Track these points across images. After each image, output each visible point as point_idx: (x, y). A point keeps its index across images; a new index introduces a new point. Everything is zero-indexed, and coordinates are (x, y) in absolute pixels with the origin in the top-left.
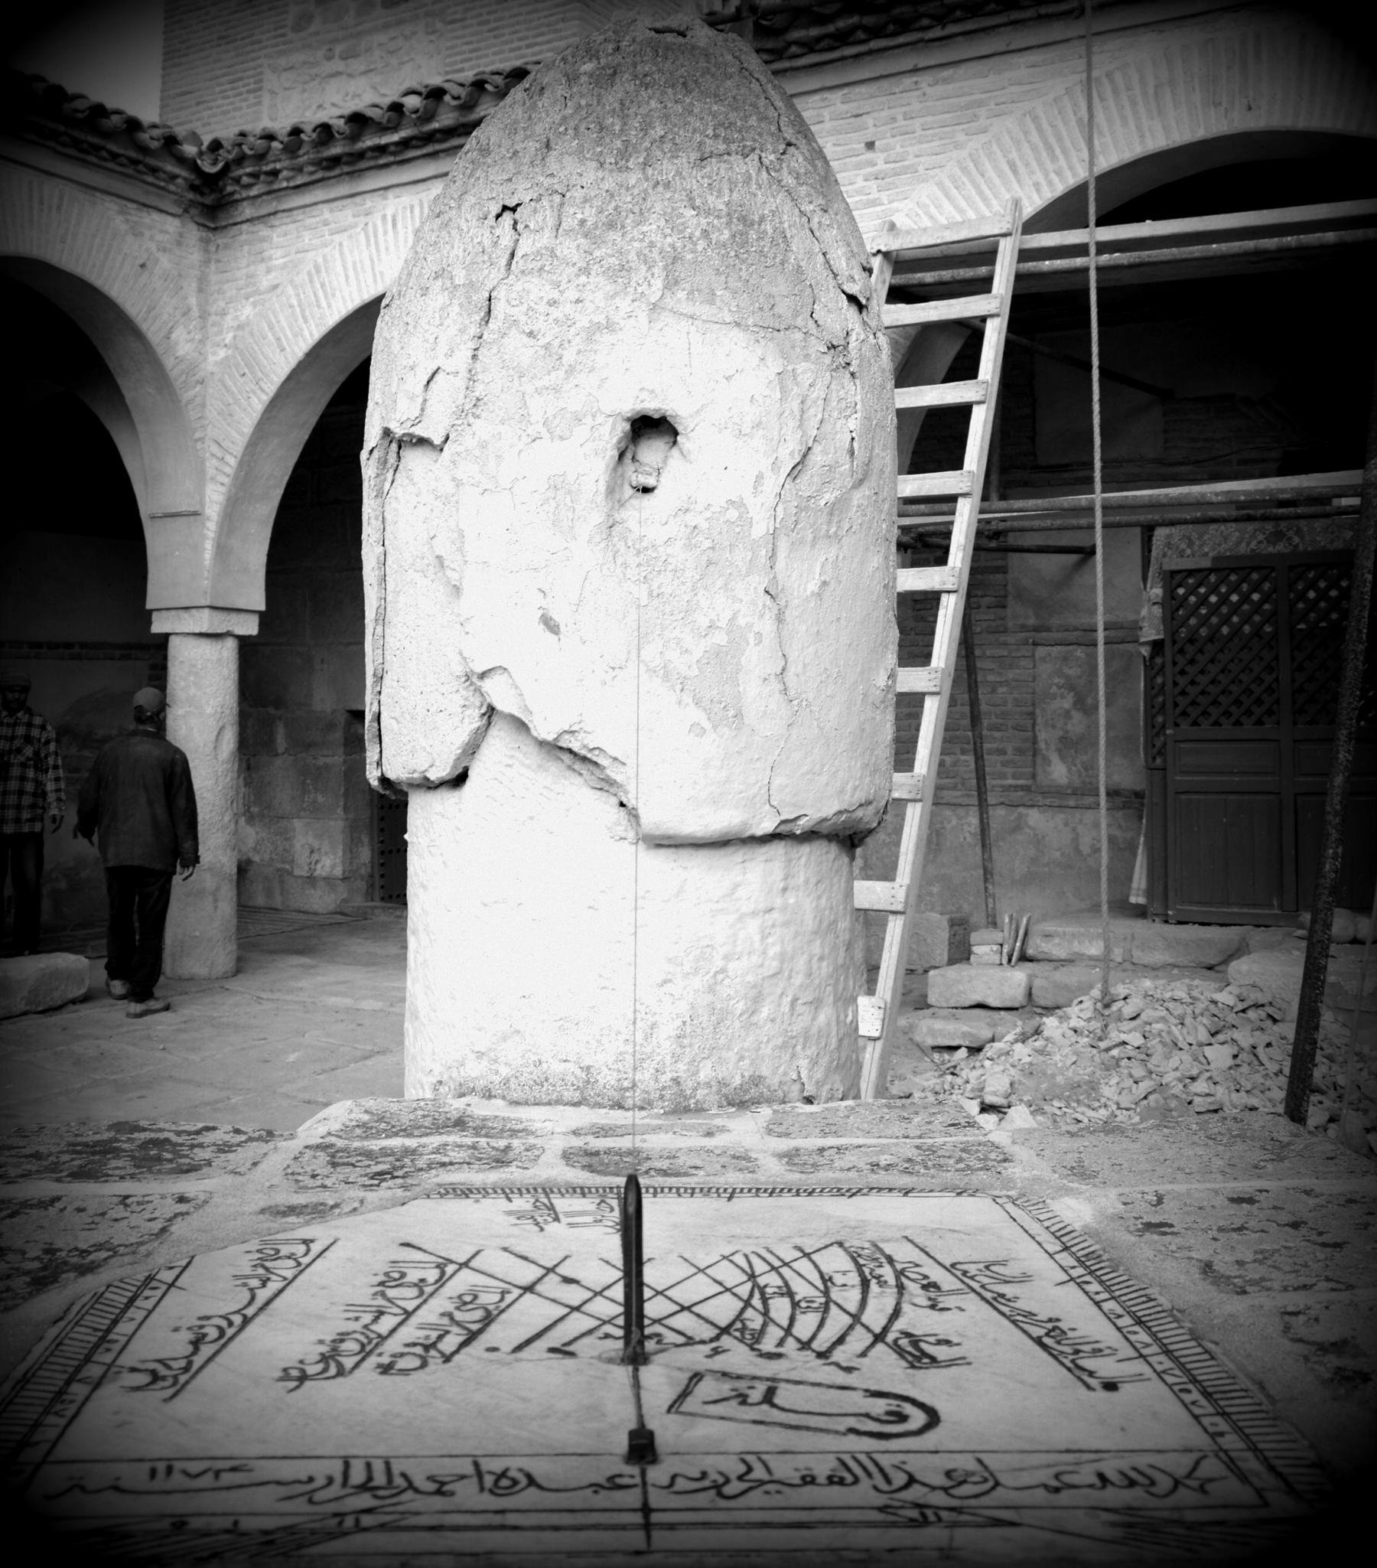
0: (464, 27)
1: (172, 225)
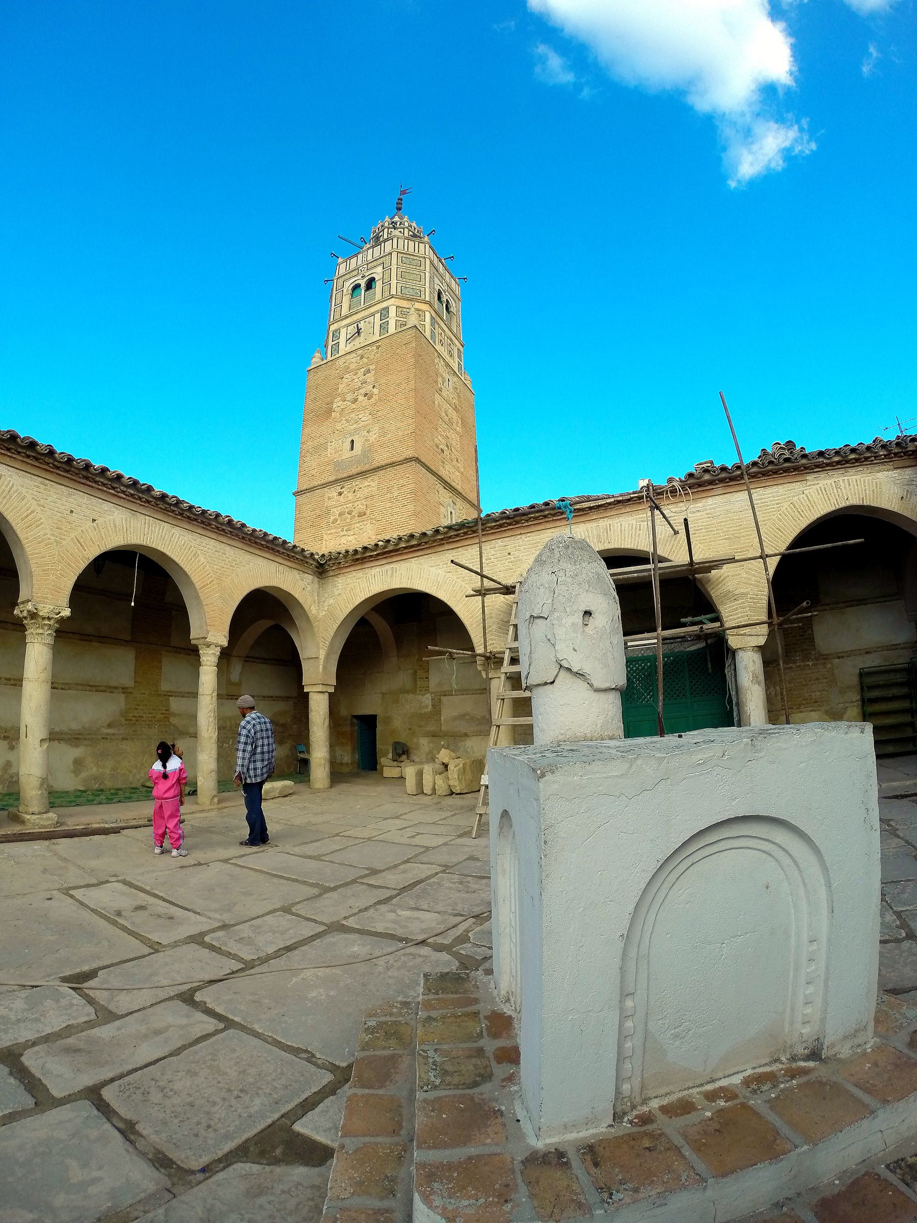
1: (311, 577)
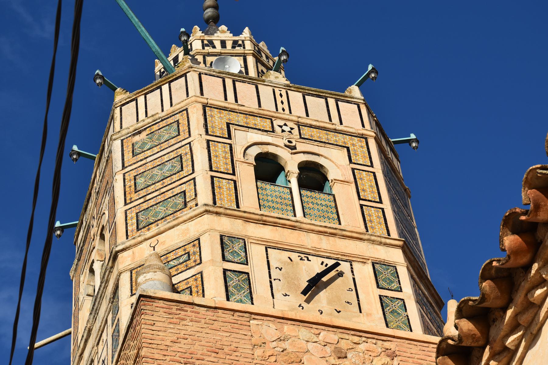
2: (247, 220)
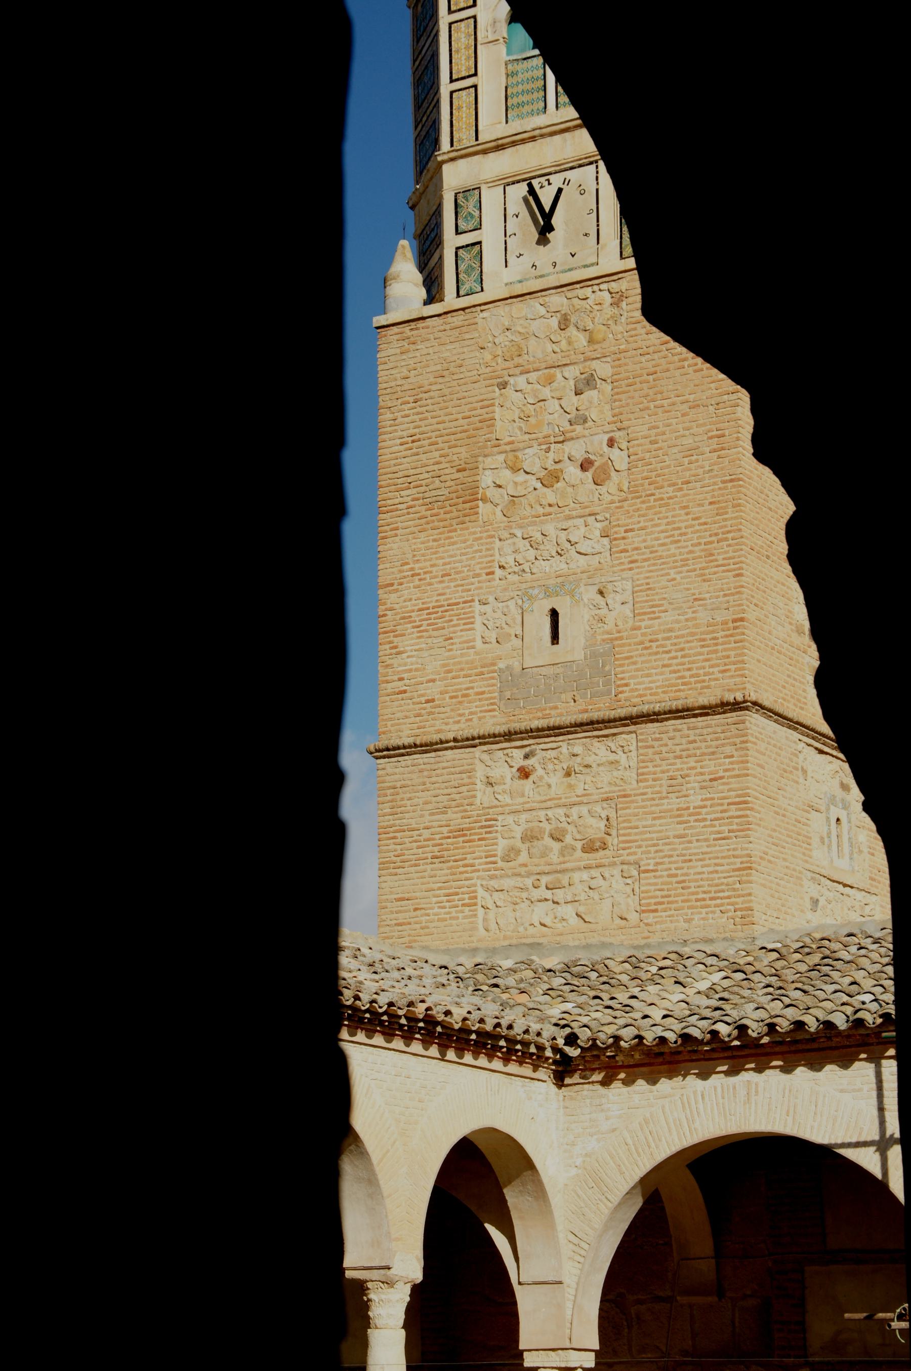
0: (655, 877)
2: (485, 152)
